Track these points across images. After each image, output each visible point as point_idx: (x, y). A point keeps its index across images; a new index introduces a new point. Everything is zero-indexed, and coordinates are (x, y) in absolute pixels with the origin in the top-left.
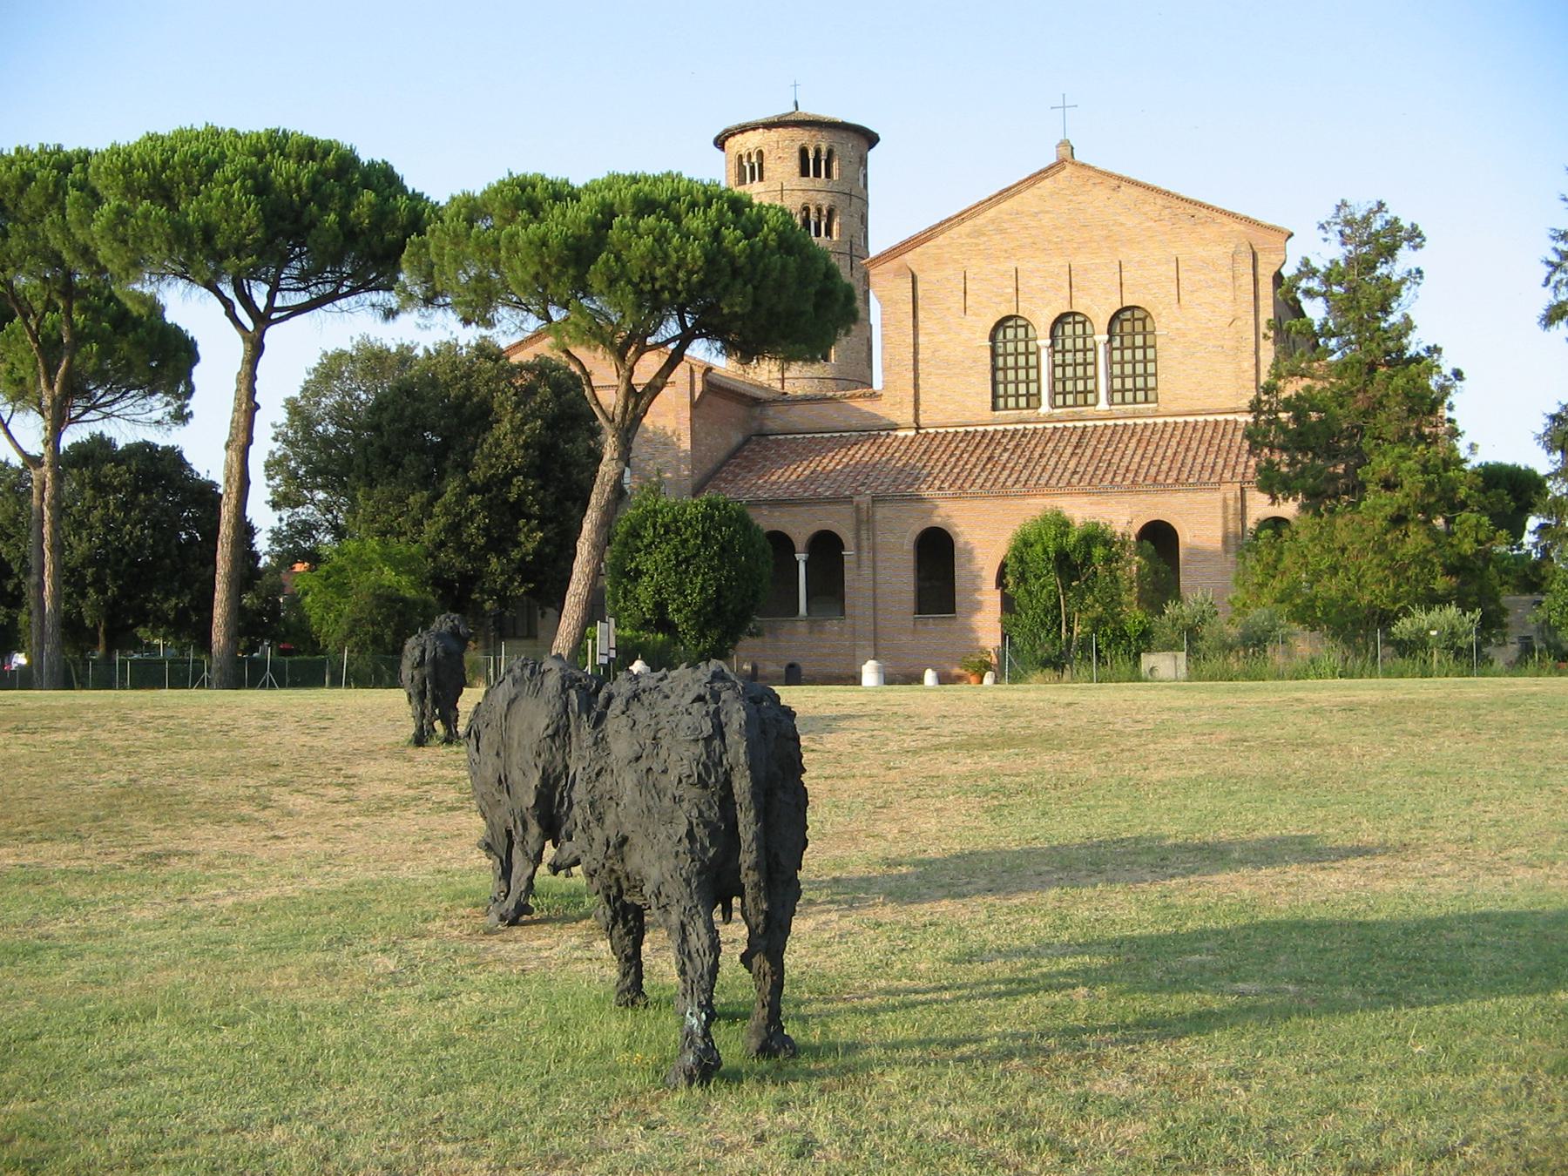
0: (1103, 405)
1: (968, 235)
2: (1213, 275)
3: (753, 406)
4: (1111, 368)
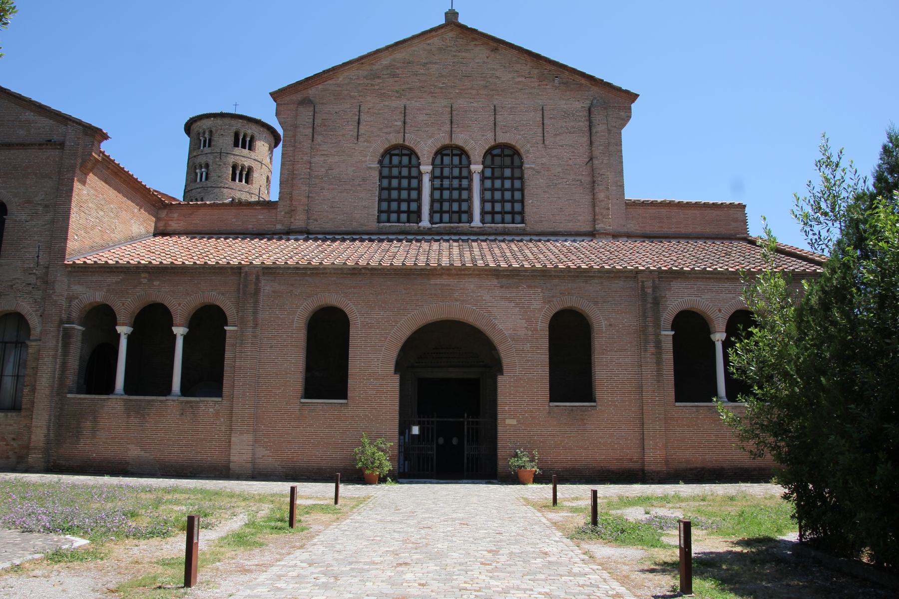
0: (477, 222)
2: (572, 124)
3: (160, 209)
4: (483, 194)
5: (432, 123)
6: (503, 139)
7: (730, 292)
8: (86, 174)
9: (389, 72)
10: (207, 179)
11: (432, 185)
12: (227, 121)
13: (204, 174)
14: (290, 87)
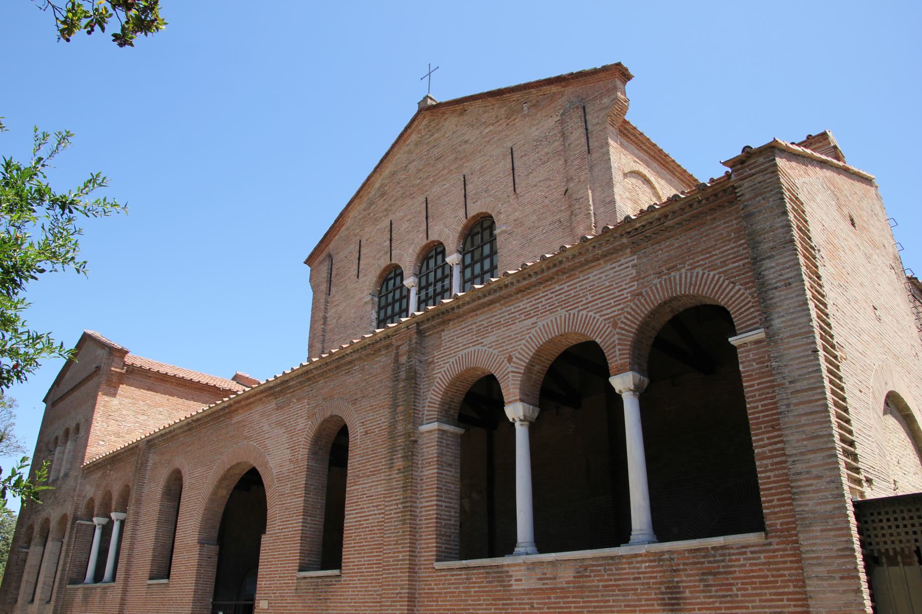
1: (364, 210)
5: (412, 228)
6: (474, 210)
7: (528, 316)
8: (116, 388)
9: (380, 193)
11: (419, 298)
14: (316, 249)
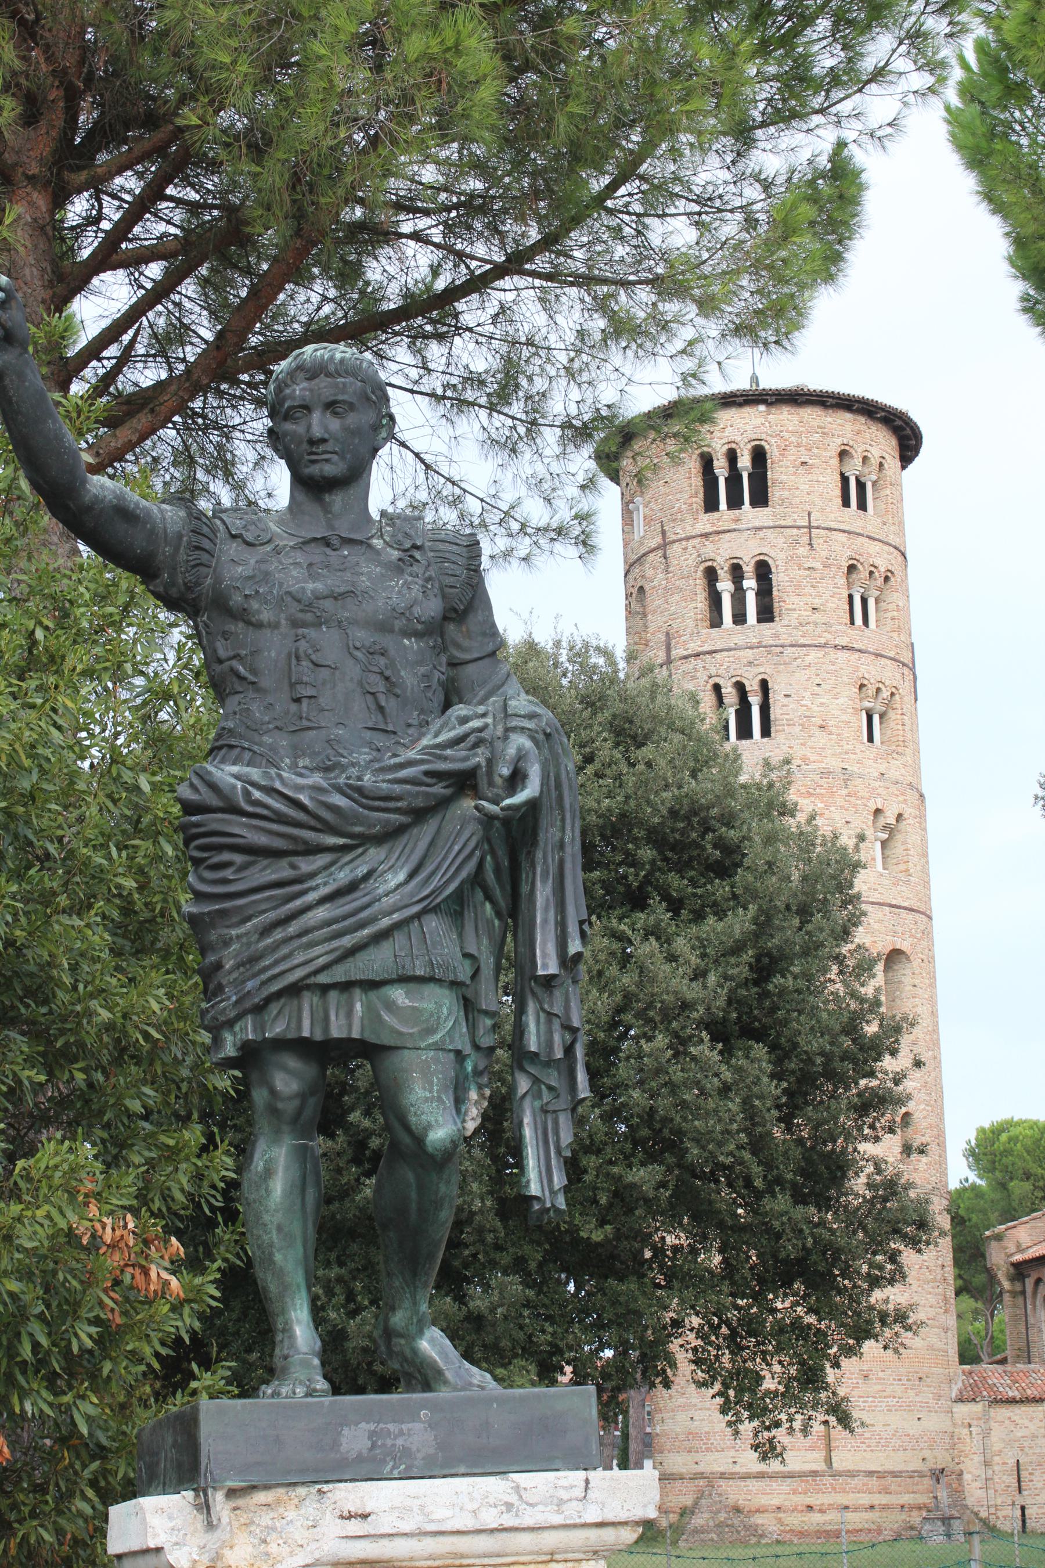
10: (766, 614)
12: (811, 415)
13: (751, 599)
